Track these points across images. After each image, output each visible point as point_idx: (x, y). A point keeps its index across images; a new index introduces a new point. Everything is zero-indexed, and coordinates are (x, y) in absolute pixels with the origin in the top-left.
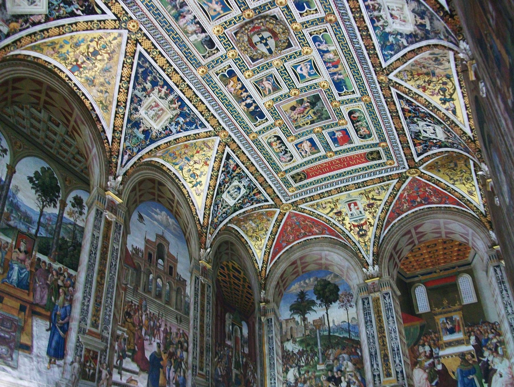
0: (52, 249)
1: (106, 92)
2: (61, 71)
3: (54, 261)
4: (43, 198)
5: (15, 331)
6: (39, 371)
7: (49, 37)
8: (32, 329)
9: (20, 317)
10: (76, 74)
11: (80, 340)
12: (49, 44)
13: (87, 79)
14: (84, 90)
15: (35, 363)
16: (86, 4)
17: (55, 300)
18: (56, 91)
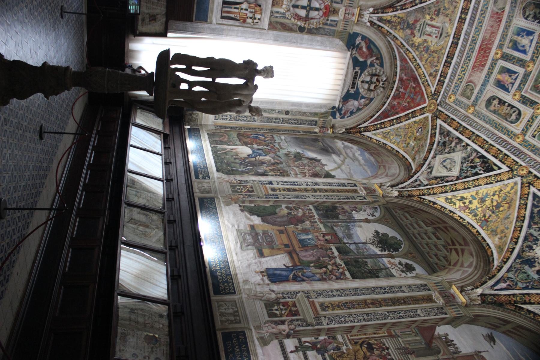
0: (348, 256)
1: (505, 236)
2: (473, 227)
3: (342, 259)
4: (376, 242)
5: (267, 244)
6: (249, 265)
7: (456, 190)
8: (277, 255)
9: (280, 245)
10: (484, 228)
11: (298, 295)
12: (459, 198)
13: (492, 231)
14: (489, 241)
15: (254, 261)
16: (487, 165)
17: (313, 266)
18: (458, 232)
